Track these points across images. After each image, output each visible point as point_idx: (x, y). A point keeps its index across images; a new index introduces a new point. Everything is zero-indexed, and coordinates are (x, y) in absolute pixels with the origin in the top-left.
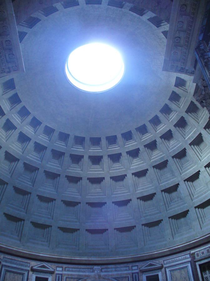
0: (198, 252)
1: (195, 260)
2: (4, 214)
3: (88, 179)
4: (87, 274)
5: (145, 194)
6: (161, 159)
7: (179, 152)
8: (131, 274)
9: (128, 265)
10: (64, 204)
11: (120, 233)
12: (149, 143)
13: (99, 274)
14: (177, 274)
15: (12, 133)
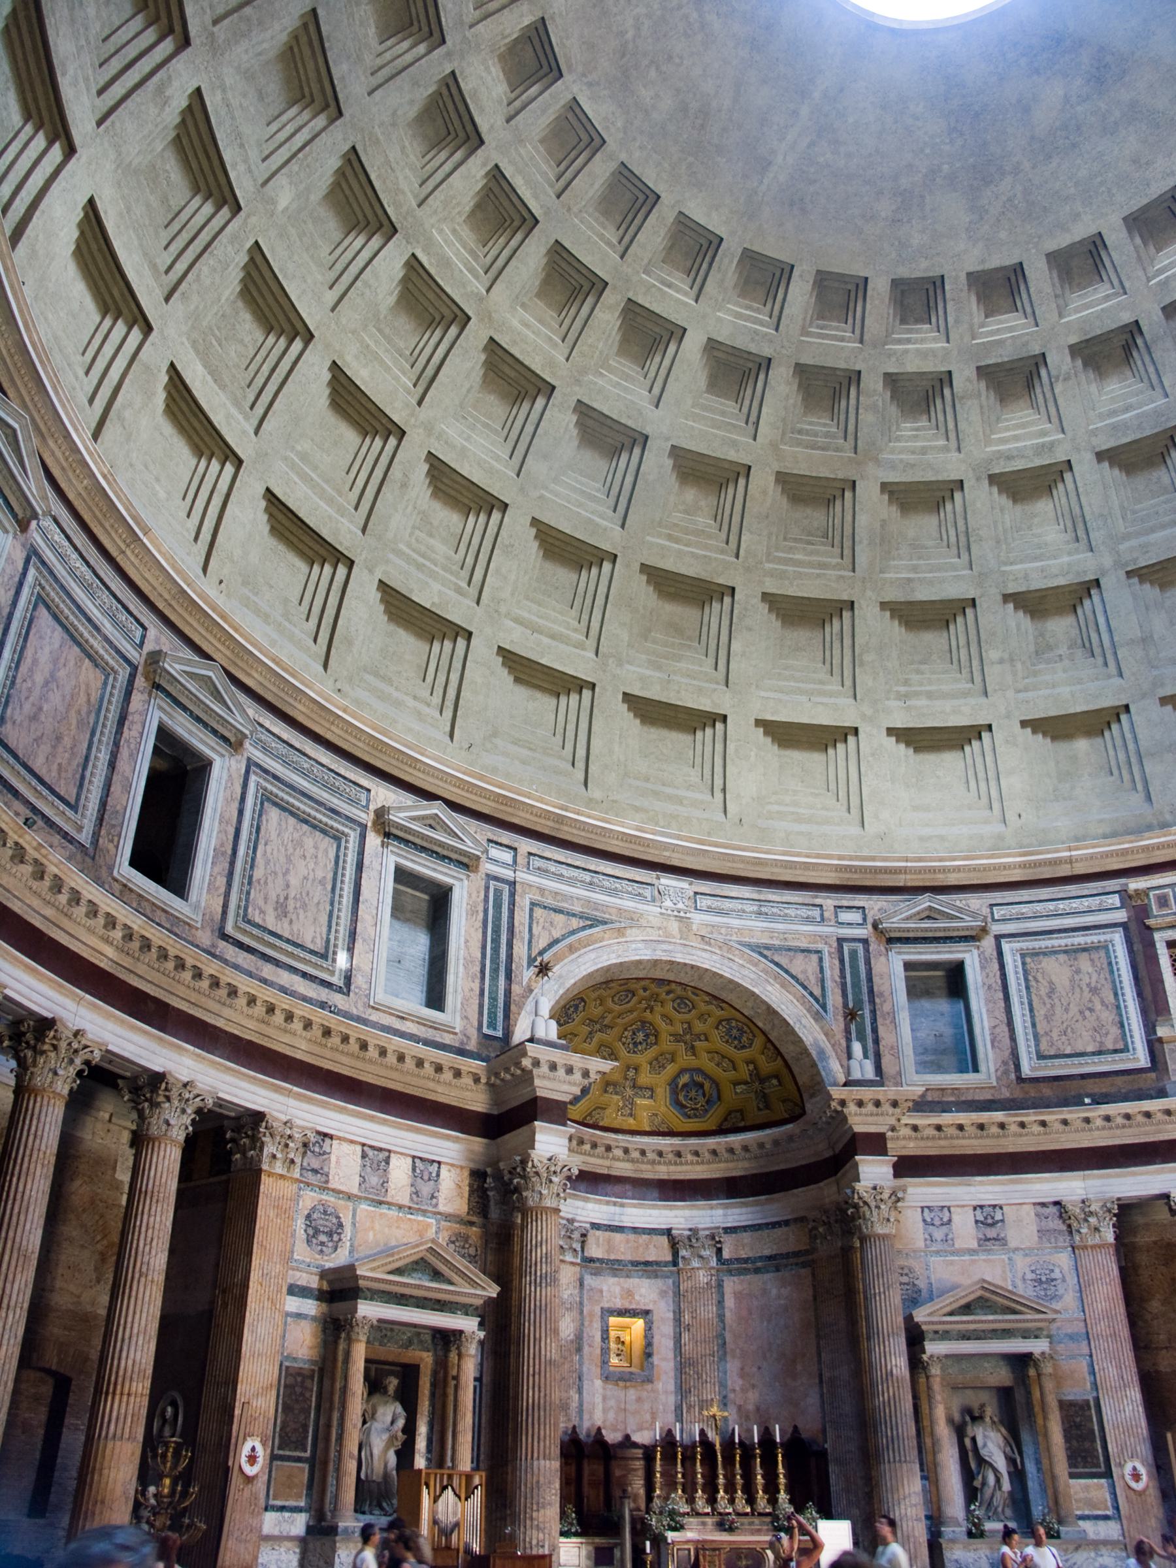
0: (1168, 890)
1: (1151, 922)
2: (269, 494)
3: (677, 453)
4: (628, 904)
5: (923, 594)
6: (1040, 449)
7: (1139, 436)
8: (835, 945)
9: (818, 901)
10: (536, 544)
11: (776, 747)
12: (1006, 359)
13: (682, 914)
14: (1056, 970)
15: (408, 58)
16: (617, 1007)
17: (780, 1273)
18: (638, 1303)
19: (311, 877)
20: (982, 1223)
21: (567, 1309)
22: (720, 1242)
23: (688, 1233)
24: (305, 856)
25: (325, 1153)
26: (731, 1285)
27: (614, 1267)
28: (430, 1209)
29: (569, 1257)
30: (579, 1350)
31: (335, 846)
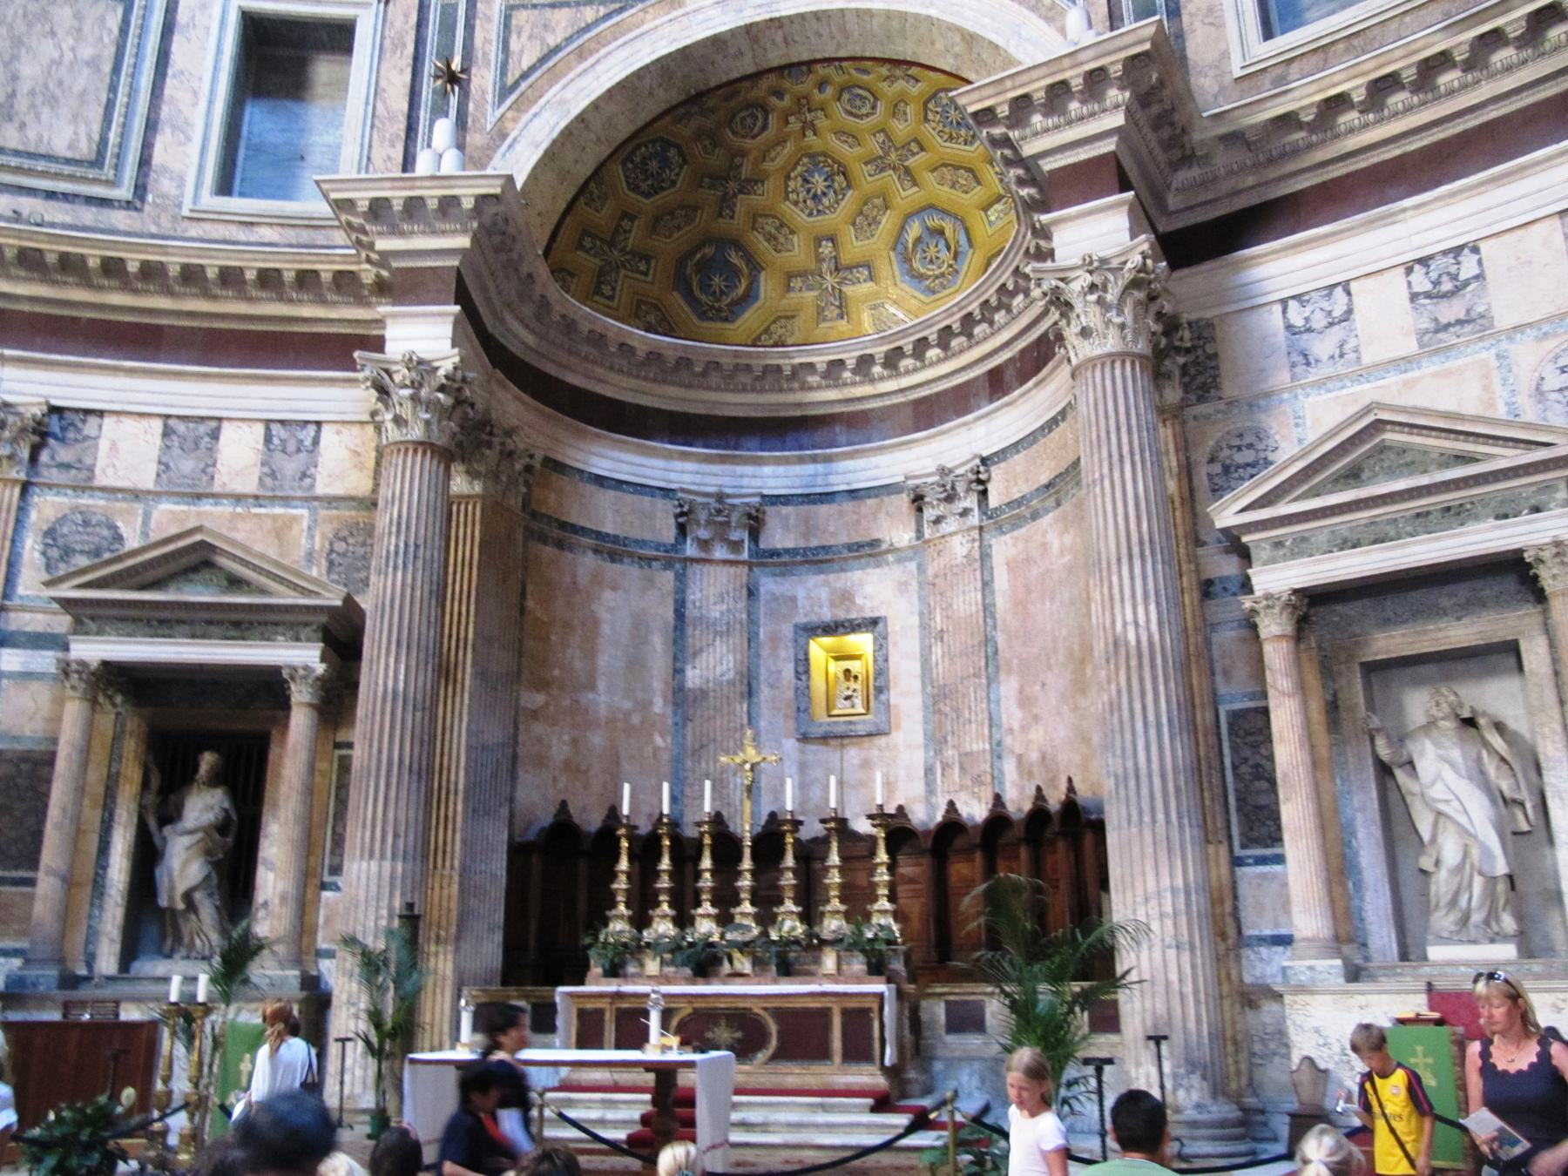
16: (748, 143)
17: (1061, 509)
18: (862, 609)
19: (69, 56)
20: (1428, 295)
21: (721, 634)
22: (980, 482)
23: (936, 478)
24: (53, 33)
25: (87, 438)
26: (1003, 548)
27: (817, 559)
28: (300, 494)
29: (720, 552)
30: (750, 693)
31: (120, 11)
